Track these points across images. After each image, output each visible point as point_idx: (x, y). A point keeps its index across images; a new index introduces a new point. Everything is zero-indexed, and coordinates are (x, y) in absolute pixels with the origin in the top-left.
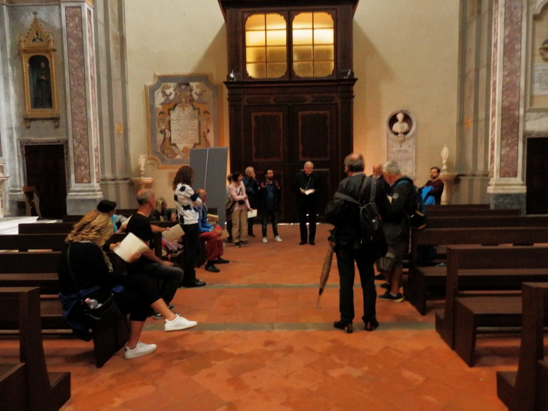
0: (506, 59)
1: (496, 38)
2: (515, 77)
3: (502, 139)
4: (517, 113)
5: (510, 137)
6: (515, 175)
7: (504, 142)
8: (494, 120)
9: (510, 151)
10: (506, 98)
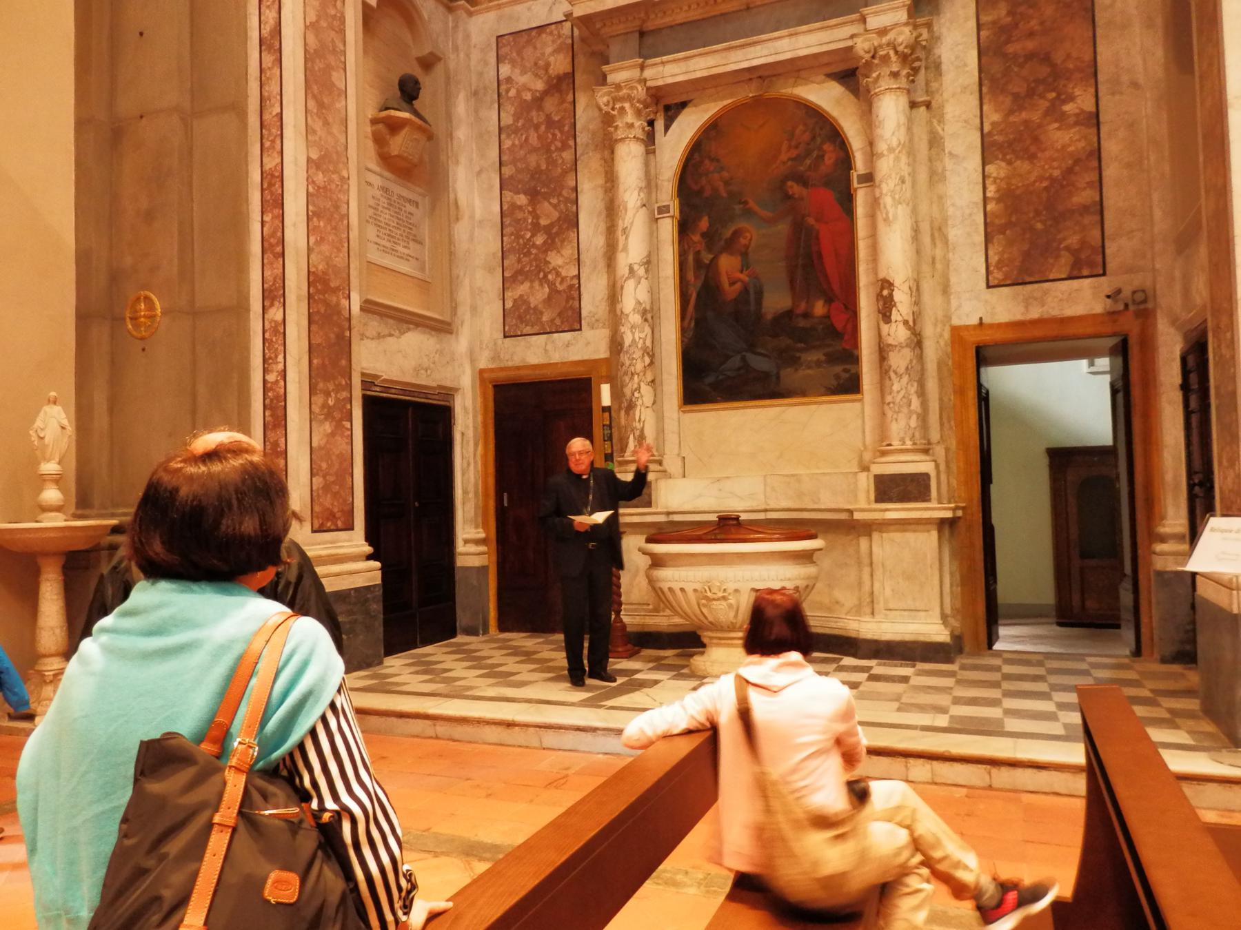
0: (312, 104)
1: (270, 15)
2: (335, 177)
3: (312, 390)
4: (345, 302)
5: (331, 387)
6: (350, 528)
7: (319, 400)
8: (276, 314)
9: (333, 434)
10: (317, 243)
